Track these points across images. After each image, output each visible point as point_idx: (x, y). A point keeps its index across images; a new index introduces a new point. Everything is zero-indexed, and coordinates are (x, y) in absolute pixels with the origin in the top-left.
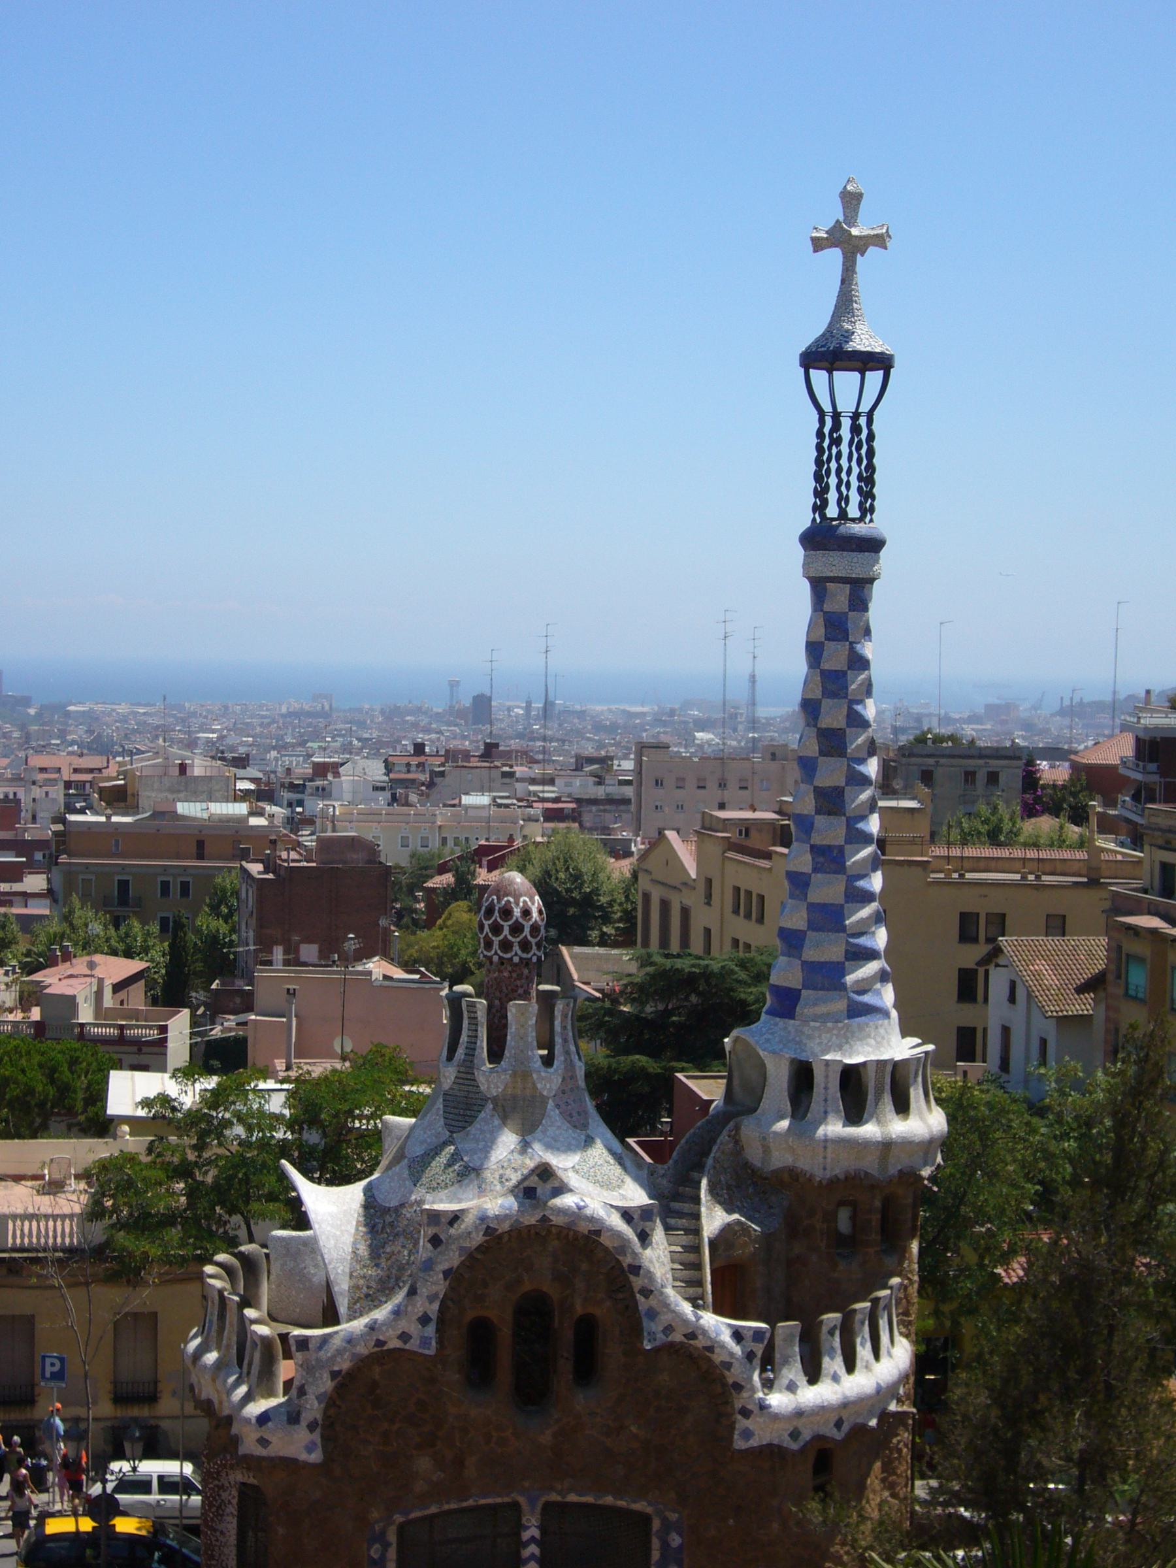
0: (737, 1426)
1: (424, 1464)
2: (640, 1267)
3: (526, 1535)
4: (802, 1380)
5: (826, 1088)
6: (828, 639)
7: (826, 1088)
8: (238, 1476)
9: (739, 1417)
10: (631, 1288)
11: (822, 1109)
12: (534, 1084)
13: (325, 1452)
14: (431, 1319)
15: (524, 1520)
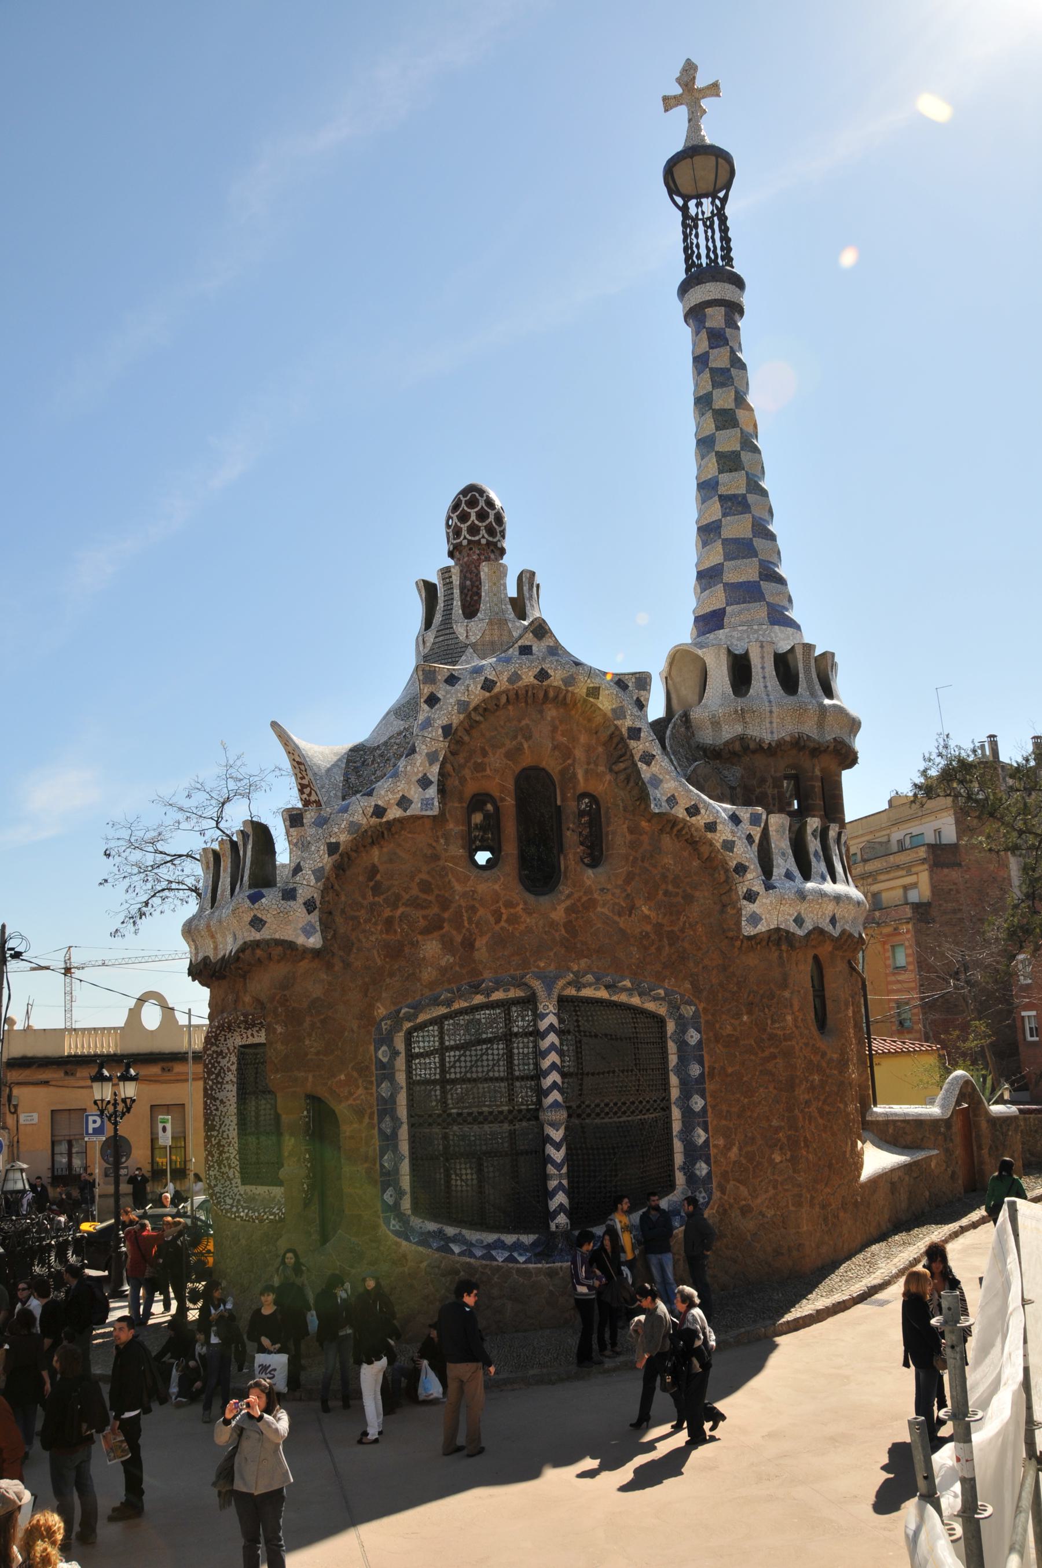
0: (744, 912)
1: (431, 948)
2: (640, 729)
3: (543, 1025)
4: (797, 873)
5: (763, 668)
6: (711, 348)
7: (763, 668)
8: (237, 1040)
9: (745, 902)
10: (632, 756)
11: (762, 685)
12: (510, 632)
13: (324, 938)
14: (431, 782)
15: (541, 1007)
